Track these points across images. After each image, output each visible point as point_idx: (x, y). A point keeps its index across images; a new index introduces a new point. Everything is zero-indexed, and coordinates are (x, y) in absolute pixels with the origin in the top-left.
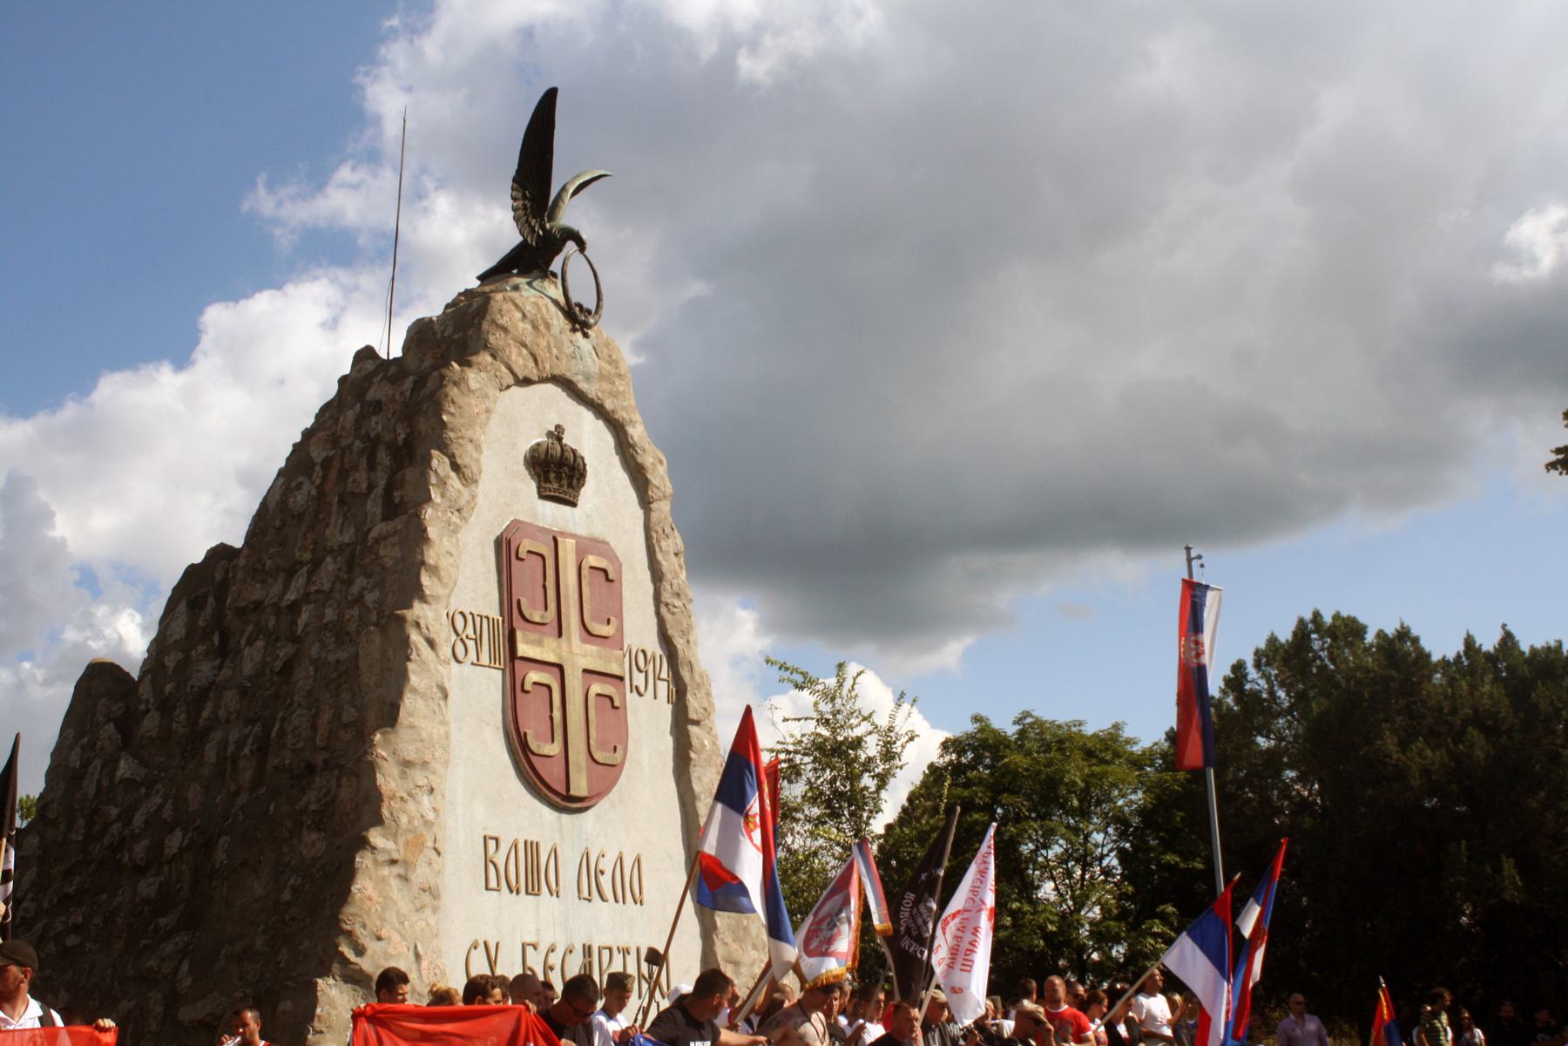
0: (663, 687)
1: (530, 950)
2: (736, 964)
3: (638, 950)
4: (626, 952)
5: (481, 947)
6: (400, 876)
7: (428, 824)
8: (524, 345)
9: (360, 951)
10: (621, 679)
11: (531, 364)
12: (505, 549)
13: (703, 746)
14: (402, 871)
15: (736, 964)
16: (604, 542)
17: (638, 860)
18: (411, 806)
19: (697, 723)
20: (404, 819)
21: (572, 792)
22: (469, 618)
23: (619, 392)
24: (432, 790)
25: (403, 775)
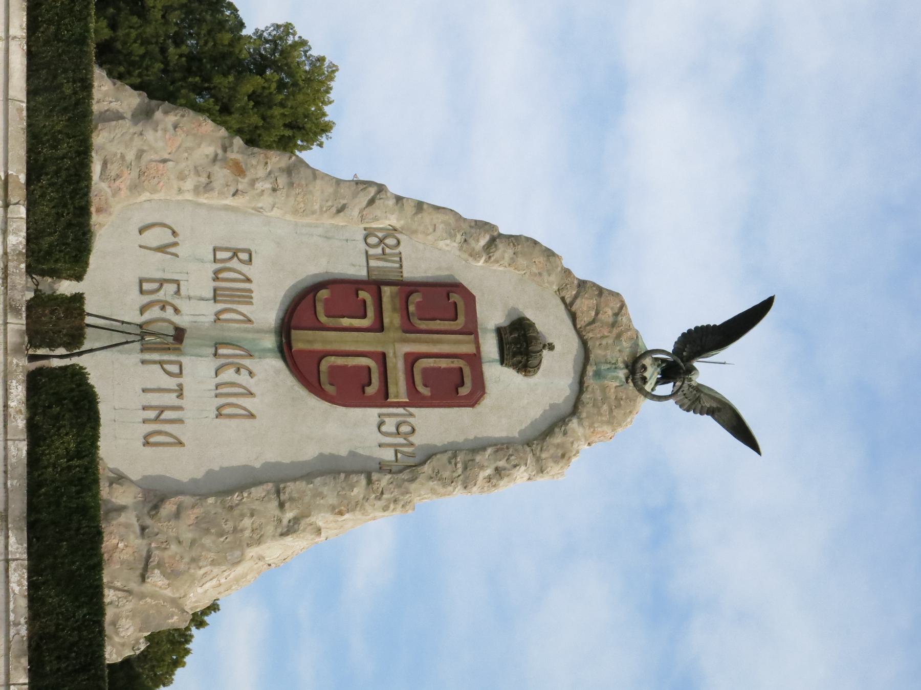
0: (388, 455)
1: (172, 288)
2: (177, 515)
3: (180, 408)
5: (172, 239)
6: (216, 155)
7: (253, 183)
8: (597, 314)
9: (166, 113)
11: (587, 319)
13: (352, 488)
14: (220, 157)
15: (177, 515)
16: (484, 393)
17: (252, 416)
18: (261, 172)
19: (369, 482)
20: (254, 162)
21: (293, 332)
22: (397, 251)
23: (599, 408)
24: (274, 190)
25: (281, 170)
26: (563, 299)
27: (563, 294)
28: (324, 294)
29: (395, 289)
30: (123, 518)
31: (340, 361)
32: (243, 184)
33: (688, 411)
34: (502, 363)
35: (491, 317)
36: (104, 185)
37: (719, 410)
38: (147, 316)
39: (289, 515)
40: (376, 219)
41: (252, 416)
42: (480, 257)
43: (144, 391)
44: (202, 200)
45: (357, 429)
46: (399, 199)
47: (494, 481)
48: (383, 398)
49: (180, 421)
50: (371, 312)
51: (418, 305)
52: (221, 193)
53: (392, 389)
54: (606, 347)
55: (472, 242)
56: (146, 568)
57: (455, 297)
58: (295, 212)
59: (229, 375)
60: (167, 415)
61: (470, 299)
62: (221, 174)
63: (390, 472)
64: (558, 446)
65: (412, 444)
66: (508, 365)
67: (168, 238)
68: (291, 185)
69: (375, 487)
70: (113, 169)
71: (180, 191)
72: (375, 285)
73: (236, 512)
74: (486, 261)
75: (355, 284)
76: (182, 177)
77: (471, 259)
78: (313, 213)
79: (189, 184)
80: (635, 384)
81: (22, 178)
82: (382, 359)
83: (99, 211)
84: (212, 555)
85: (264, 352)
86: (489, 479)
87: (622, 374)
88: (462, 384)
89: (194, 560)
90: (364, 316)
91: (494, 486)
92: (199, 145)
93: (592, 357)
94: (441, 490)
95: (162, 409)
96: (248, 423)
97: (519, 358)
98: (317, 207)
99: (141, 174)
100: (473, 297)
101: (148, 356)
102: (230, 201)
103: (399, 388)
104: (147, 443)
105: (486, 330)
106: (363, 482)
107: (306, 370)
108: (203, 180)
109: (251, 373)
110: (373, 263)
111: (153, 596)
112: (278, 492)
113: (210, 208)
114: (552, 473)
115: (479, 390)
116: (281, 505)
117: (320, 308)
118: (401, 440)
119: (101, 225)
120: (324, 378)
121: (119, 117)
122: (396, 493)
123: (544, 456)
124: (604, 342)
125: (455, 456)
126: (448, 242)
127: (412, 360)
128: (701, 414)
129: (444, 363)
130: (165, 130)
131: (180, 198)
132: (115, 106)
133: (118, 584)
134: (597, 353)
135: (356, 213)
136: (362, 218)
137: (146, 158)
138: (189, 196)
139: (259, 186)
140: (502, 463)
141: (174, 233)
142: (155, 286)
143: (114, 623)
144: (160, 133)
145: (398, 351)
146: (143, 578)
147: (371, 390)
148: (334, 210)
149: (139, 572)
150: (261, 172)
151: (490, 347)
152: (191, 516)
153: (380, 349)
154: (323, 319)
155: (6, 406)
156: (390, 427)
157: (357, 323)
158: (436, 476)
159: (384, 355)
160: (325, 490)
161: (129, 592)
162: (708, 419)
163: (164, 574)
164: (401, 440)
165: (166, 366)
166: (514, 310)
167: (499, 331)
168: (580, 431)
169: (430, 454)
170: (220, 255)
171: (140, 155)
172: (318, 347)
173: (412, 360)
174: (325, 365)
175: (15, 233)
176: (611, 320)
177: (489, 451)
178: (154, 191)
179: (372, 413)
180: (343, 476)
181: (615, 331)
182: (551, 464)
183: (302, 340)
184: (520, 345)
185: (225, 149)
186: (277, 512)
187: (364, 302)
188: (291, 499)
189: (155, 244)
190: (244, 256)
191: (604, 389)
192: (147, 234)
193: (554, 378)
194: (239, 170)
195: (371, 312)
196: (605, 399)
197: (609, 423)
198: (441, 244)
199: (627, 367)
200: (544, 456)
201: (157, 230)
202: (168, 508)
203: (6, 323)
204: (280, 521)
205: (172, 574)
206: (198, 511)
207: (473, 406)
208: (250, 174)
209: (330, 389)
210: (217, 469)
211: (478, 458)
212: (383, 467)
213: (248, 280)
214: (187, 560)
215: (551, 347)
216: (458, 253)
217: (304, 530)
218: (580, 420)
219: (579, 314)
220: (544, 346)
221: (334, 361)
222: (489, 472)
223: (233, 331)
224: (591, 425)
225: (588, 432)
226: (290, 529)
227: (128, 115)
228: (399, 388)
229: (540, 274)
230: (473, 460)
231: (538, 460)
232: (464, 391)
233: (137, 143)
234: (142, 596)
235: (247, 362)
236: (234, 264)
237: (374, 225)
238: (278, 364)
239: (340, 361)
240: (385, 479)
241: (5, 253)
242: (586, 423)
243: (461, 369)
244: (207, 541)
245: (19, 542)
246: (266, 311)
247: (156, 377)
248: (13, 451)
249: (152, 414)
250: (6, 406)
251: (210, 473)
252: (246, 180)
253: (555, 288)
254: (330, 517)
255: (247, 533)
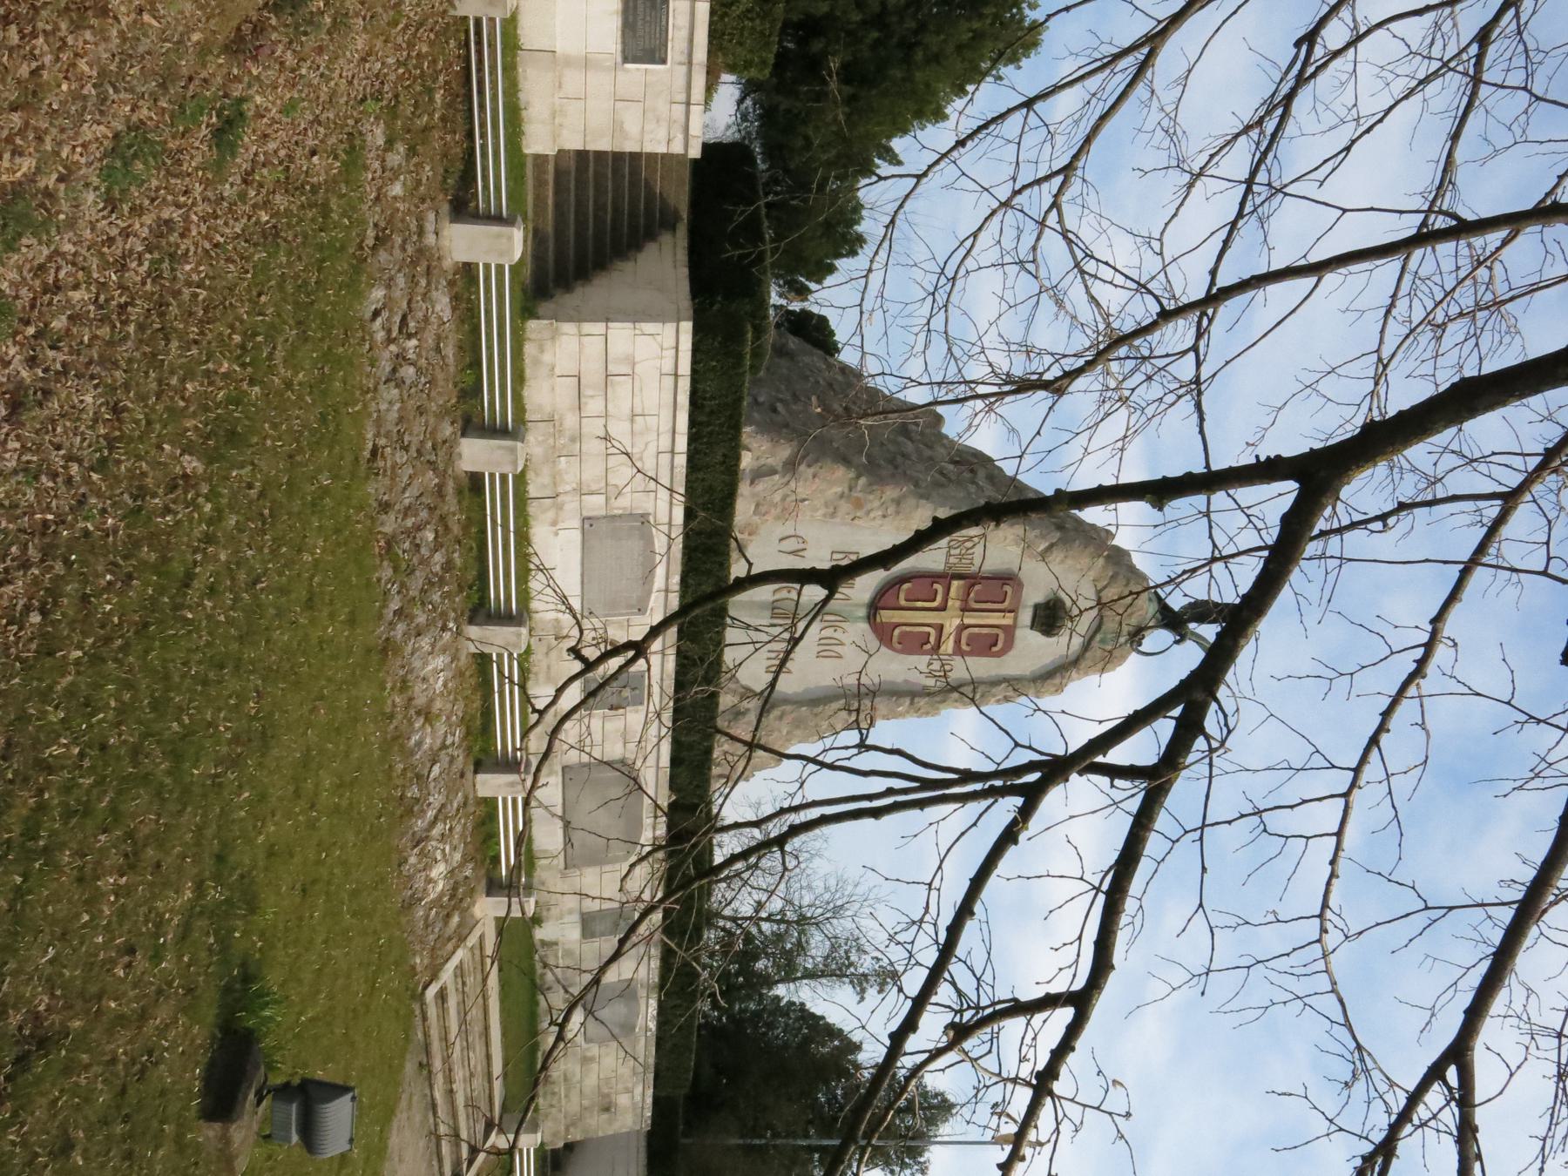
2: (781, 718)
7: (868, 513)
9: (809, 466)
12: (1007, 579)
18: (876, 504)
19: (912, 703)
28: (906, 586)
29: (961, 582)
30: (746, 719)
35: (1034, 595)
38: (778, 596)
50: (939, 598)
51: (977, 593)
57: (1008, 588)
59: (829, 632)
61: (1020, 585)
62: (845, 507)
63: (929, 694)
67: (801, 546)
68: (898, 513)
70: (763, 509)
82: (940, 628)
85: (857, 619)
88: (995, 644)
99: (784, 509)
103: (948, 646)
107: (884, 634)
115: (1009, 644)
117: (902, 596)
120: (895, 639)
121: (773, 472)
127: (963, 627)
129: (985, 631)
132: (770, 461)
145: (951, 623)
150: (876, 504)
151: (1026, 616)
152: (788, 719)
170: (836, 556)
174: (897, 632)
183: (886, 616)
184: (1050, 617)
185: (850, 489)
194: (858, 504)
195: (939, 598)
208: (869, 506)
209: (899, 647)
212: (926, 693)
227: (779, 468)
228: (948, 646)
232: (994, 649)
238: (864, 626)
244: (798, 732)
251: (806, 691)
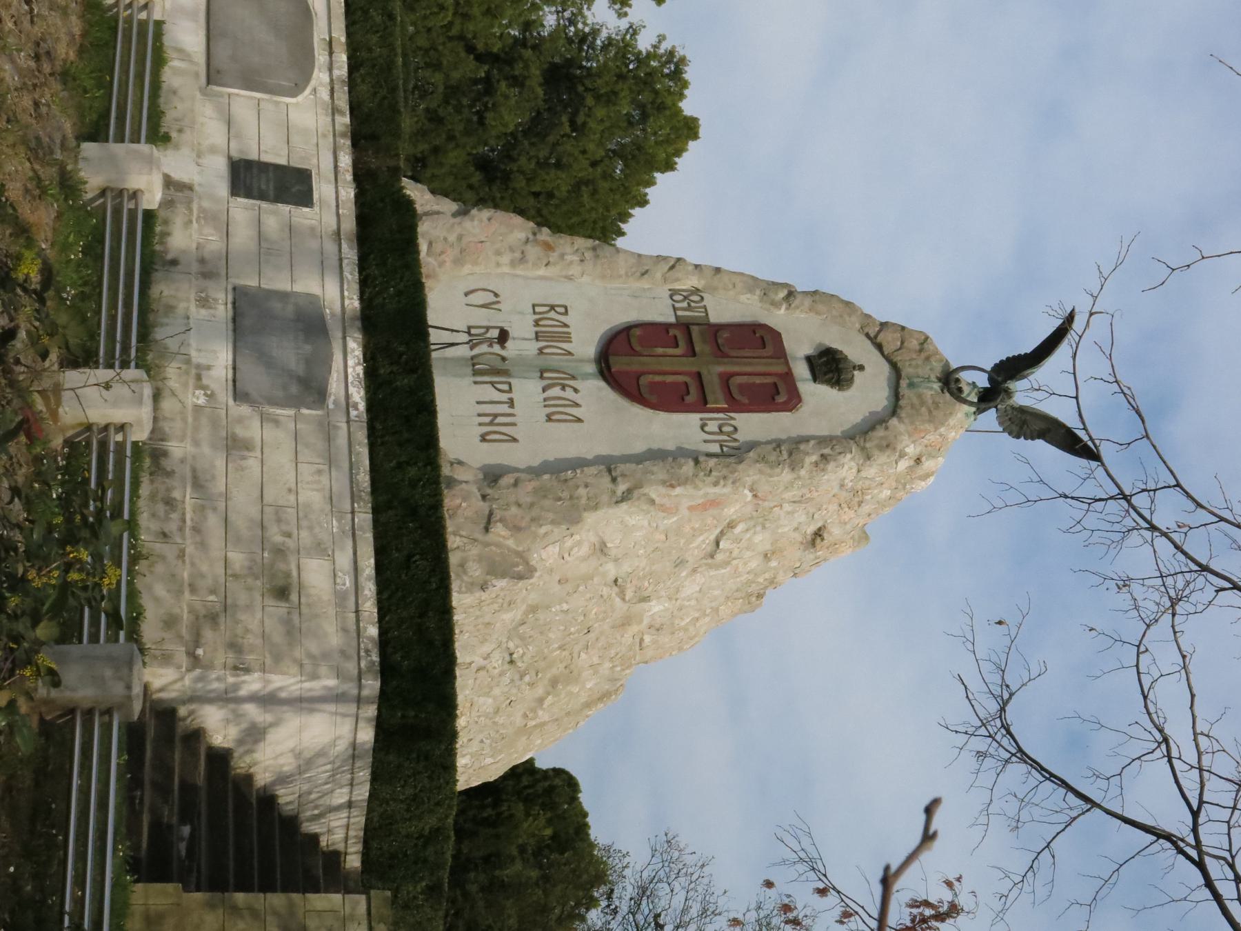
0: (715, 448)
4: (511, 403)
5: (495, 299)
8: (902, 343)
10: (706, 403)
13: (680, 467)
17: (579, 420)
18: (568, 249)
26: (867, 335)
27: (866, 330)
31: (658, 378)
32: (554, 256)
33: (1018, 437)
34: (815, 380)
36: (430, 260)
37: (1049, 430)
38: (476, 351)
39: (622, 487)
40: (677, 280)
41: (579, 420)
42: (781, 305)
43: (478, 403)
44: (519, 272)
45: (682, 428)
46: (697, 266)
47: (821, 466)
48: (702, 405)
49: (514, 424)
52: (534, 264)
53: (710, 397)
54: (917, 366)
55: (772, 295)
56: (489, 522)
58: (603, 277)
59: (556, 392)
60: (500, 420)
61: (776, 336)
62: (533, 251)
64: (882, 438)
65: (736, 440)
66: (822, 382)
67: (492, 298)
69: (703, 466)
70: (438, 247)
71: (498, 265)
72: (685, 326)
73: (571, 483)
74: (787, 309)
75: (666, 327)
76: (498, 253)
77: (772, 308)
78: (620, 276)
79: (506, 259)
80: (952, 394)
81: (343, 39)
83: (428, 277)
84: (551, 516)
85: (586, 376)
86: (816, 464)
87: (937, 386)
89: (533, 520)
90: (677, 346)
91: (823, 470)
92: (512, 232)
93: (903, 374)
94: (768, 471)
95: (496, 416)
96: (576, 425)
97: (830, 375)
98: (622, 272)
100: (779, 334)
101: (479, 379)
102: (542, 272)
104: (483, 438)
105: (795, 358)
106: (691, 463)
108: (518, 255)
109: (576, 391)
110: (680, 313)
111: (498, 545)
112: (610, 471)
113: (526, 278)
114: (879, 461)
116: (614, 480)
118: (726, 438)
119: (431, 289)
122: (725, 472)
123: (868, 445)
124: (914, 363)
125: (779, 446)
126: (749, 296)
127: (726, 379)
128: (1033, 439)
129: (758, 380)
130: (481, 221)
131: (499, 271)
133: (464, 533)
134: (907, 371)
135: (659, 275)
136: (665, 280)
137: (465, 241)
138: (506, 269)
139: (568, 258)
140: (827, 451)
141: (496, 295)
142: (482, 331)
143: (462, 565)
144: (476, 223)
146: (487, 529)
147: (689, 399)
148: (638, 274)
149: (482, 526)
151: (801, 371)
153: (695, 369)
154: (638, 348)
155: (336, 167)
156: (712, 426)
157: (670, 351)
158: (763, 459)
159: (699, 375)
160: (655, 469)
161: (475, 540)
162: (1040, 443)
163: (506, 526)
164: (726, 438)
165: (498, 386)
166: (820, 344)
167: (809, 359)
168: (902, 428)
169: (752, 446)
170: (538, 309)
171: (460, 238)
172: (635, 367)
173: (726, 379)
174: (644, 380)
175: (340, 68)
176: (918, 347)
177: (812, 442)
178: (475, 263)
179: (694, 418)
180: (670, 459)
181: (923, 355)
182: (876, 452)
184: (830, 367)
185: (534, 234)
186: (610, 486)
187: (675, 337)
188: (623, 475)
189: (481, 303)
190: (562, 310)
191: (920, 396)
192: (471, 296)
193: (869, 390)
194: (548, 247)
195: (682, 343)
196: (923, 403)
197: (930, 421)
198: (743, 298)
199: (940, 380)
200: (868, 445)
201: (480, 293)
202: (507, 480)
203: (333, 120)
204: (614, 492)
205: (516, 529)
206: (534, 484)
207: (790, 410)
210: (552, 459)
211: (802, 447)
213: (566, 326)
214: (528, 519)
215: (861, 368)
216: (760, 305)
217: (639, 499)
218: (900, 419)
219: (884, 344)
220: (854, 368)
221: (650, 378)
222: (814, 458)
223: (555, 361)
224: (912, 423)
225: (910, 428)
226: (626, 497)
229: (841, 316)
230: (798, 448)
231: (863, 449)
233: (458, 230)
234: (487, 545)
235: (571, 383)
236: (552, 314)
237: (677, 286)
239: (658, 378)
240: (712, 462)
241: (332, 80)
242: (906, 421)
243: (775, 384)
245: (351, 248)
246: (585, 345)
247: (489, 393)
248: (342, 193)
249: (487, 419)
250: (336, 167)
252: (555, 254)
253: (858, 326)
254: (662, 490)
255: (583, 501)
